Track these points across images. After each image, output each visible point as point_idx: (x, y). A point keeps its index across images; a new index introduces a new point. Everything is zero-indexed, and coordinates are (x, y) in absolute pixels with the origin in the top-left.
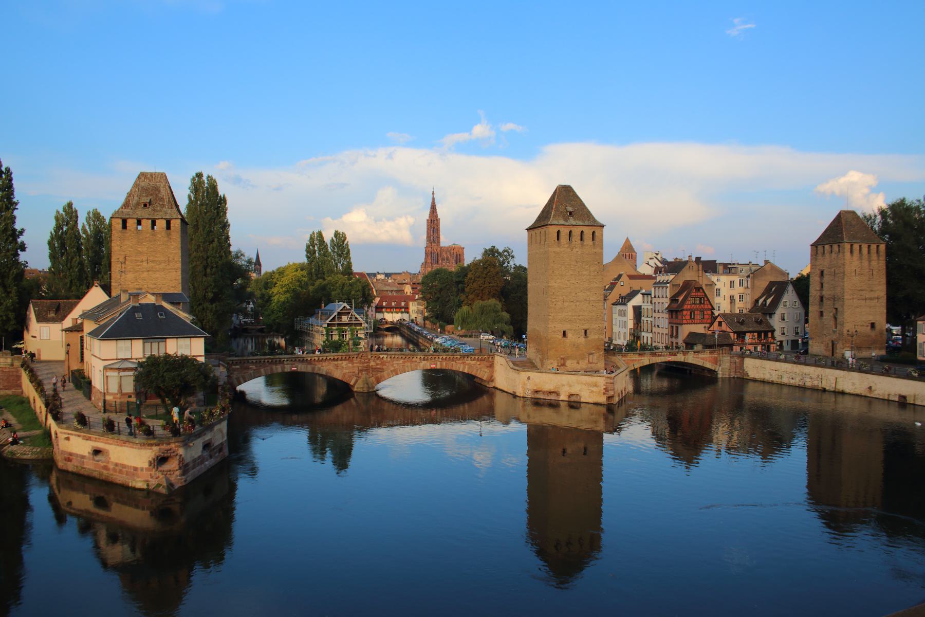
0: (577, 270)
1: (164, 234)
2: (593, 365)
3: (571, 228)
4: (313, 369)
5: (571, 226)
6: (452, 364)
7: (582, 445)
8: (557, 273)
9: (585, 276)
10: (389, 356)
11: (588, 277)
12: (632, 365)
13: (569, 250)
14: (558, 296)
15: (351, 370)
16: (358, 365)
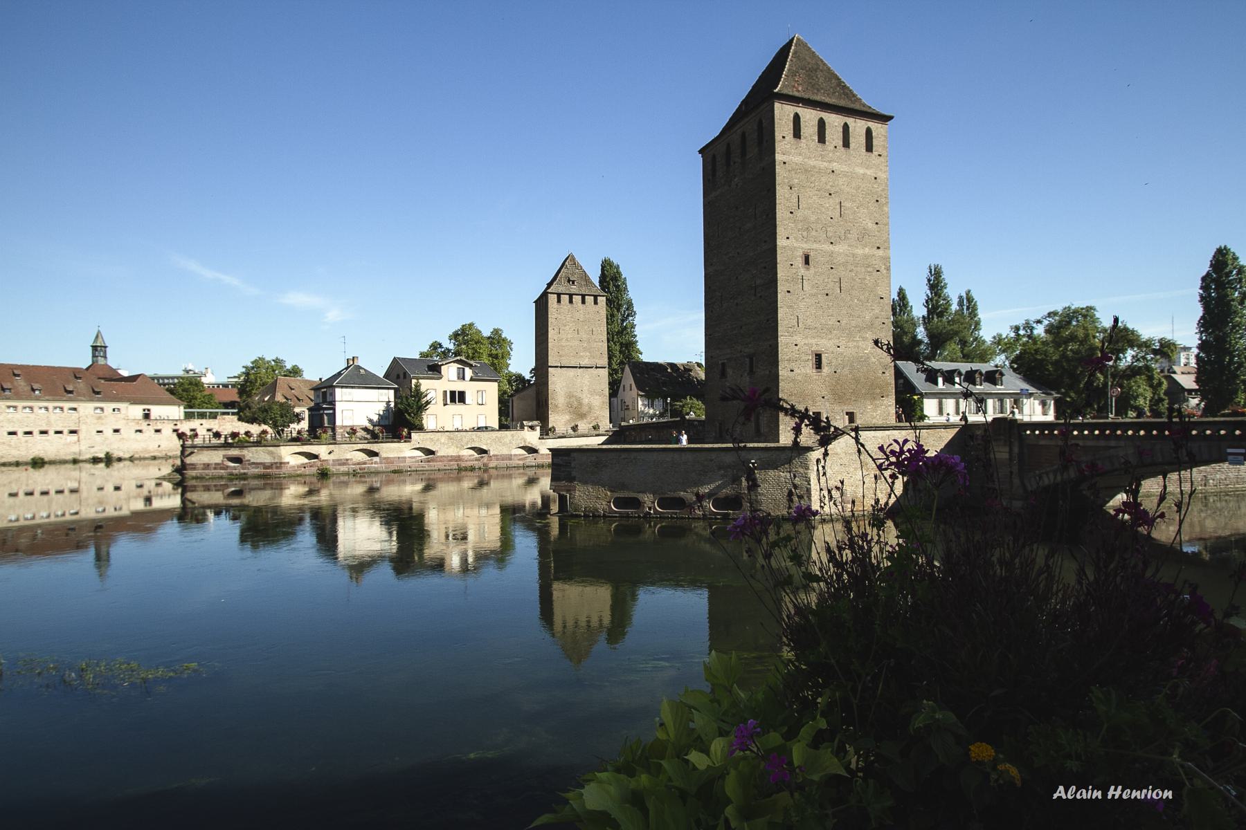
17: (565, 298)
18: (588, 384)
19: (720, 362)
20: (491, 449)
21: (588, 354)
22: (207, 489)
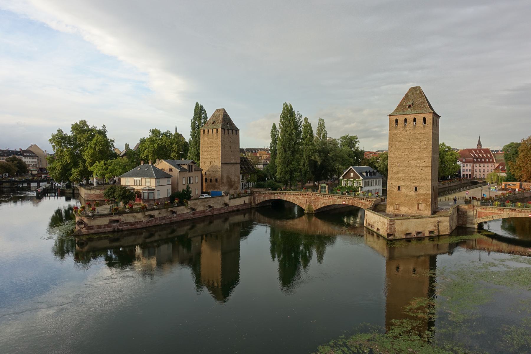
1: (216, 135)
2: (421, 212)
3: (406, 117)
4: (287, 199)
5: (406, 115)
7: (411, 267)
9: (416, 149)
10: (321, 195)
11: (419, 150)
14: (395, 163)
17: (226, 131)
18: (234, 172)
20: (214, 206)
21: (234, 158)
22: (100, 239)
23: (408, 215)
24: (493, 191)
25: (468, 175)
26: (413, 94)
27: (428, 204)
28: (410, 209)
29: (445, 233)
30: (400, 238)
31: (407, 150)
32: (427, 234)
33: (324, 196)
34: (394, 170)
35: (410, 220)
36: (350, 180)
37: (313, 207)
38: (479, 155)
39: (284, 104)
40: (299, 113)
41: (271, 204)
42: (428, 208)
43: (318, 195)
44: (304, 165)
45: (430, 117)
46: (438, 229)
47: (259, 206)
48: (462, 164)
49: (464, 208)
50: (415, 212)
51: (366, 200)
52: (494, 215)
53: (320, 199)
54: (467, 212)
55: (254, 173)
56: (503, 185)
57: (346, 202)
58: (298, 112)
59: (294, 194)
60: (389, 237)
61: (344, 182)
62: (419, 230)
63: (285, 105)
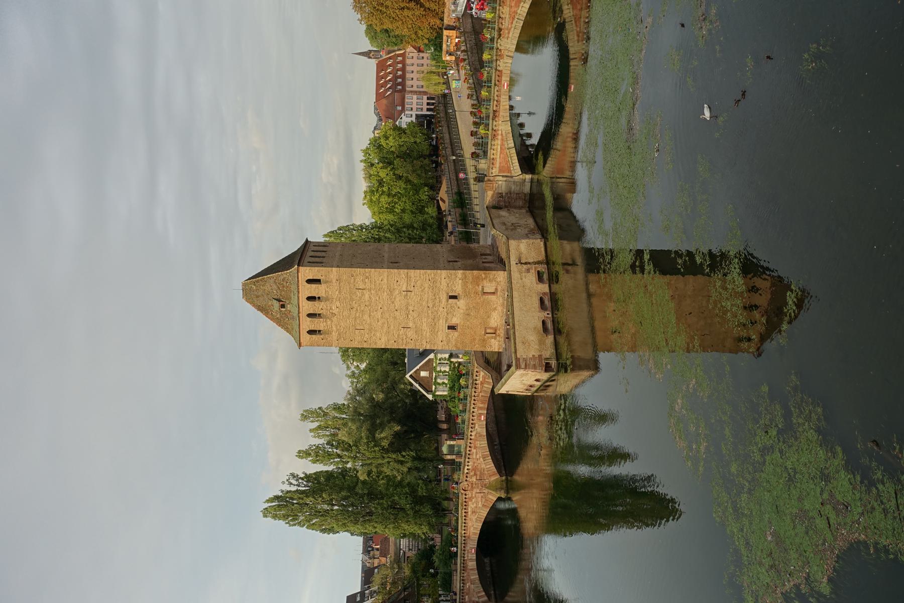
0: (362, 308)
2: (499, 288)
4: (475, 534)
5: (300, 315)
6: (482, 396)
8: (366, 335)
10: (467, 464)
11: (373, 292)
12: (508, 151)
13: (335, 319)
15: (479, 499)
16: (474, 493)
19: (447, 331)
23: (507, 315)
24: (459, 85)
25: (429, 101)
26: (258, 297)
27: (483, 275)
28: (495, 309)
29: (543, 249)
30: (553, 347)
31: (373, 312)
32: (544, 288)
33: (469, 458)
34: (414, 336)
35: (516, 323)
36: (435, 379)
37: (493, 478)
38: (390, 80)
39: (265, 516)
40: (285, 481)
41: (488, 558)
42: (491, 277)
43: (468, 469)
44: (402, 463)
45: (307, 271)
46: (535, 263)
47: (492, 592)
48: (406, 112)
49: (492, 197)
50: (501, 299)
51: (476, 376)
52: (506, 146)
53: (475, 465)
54: (500, 192)
55: (419, 585)
56: (448, 58)
57: (481, 414)
58: (283, 483)
59: (465, 520)
60: (551, 367)
61: (438, 391)
62: (537, 303)
63: (266, 513)
